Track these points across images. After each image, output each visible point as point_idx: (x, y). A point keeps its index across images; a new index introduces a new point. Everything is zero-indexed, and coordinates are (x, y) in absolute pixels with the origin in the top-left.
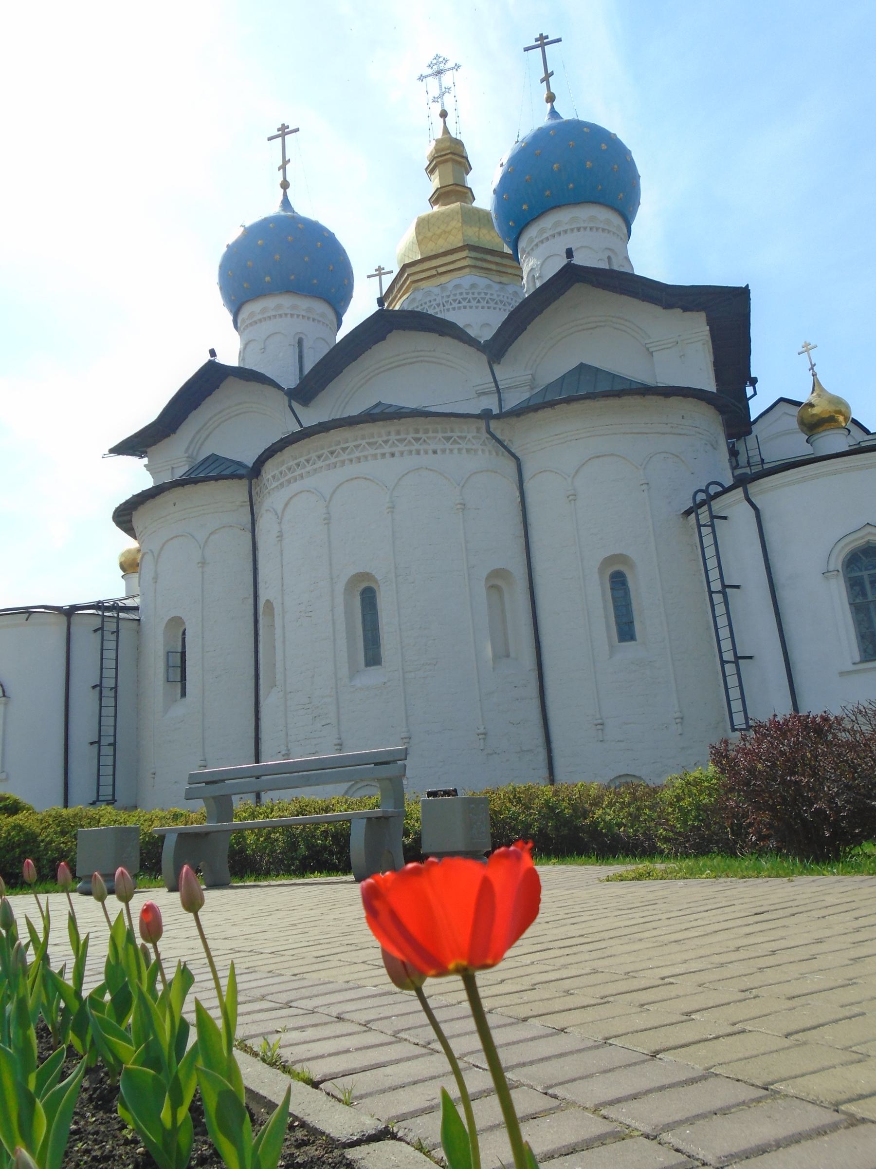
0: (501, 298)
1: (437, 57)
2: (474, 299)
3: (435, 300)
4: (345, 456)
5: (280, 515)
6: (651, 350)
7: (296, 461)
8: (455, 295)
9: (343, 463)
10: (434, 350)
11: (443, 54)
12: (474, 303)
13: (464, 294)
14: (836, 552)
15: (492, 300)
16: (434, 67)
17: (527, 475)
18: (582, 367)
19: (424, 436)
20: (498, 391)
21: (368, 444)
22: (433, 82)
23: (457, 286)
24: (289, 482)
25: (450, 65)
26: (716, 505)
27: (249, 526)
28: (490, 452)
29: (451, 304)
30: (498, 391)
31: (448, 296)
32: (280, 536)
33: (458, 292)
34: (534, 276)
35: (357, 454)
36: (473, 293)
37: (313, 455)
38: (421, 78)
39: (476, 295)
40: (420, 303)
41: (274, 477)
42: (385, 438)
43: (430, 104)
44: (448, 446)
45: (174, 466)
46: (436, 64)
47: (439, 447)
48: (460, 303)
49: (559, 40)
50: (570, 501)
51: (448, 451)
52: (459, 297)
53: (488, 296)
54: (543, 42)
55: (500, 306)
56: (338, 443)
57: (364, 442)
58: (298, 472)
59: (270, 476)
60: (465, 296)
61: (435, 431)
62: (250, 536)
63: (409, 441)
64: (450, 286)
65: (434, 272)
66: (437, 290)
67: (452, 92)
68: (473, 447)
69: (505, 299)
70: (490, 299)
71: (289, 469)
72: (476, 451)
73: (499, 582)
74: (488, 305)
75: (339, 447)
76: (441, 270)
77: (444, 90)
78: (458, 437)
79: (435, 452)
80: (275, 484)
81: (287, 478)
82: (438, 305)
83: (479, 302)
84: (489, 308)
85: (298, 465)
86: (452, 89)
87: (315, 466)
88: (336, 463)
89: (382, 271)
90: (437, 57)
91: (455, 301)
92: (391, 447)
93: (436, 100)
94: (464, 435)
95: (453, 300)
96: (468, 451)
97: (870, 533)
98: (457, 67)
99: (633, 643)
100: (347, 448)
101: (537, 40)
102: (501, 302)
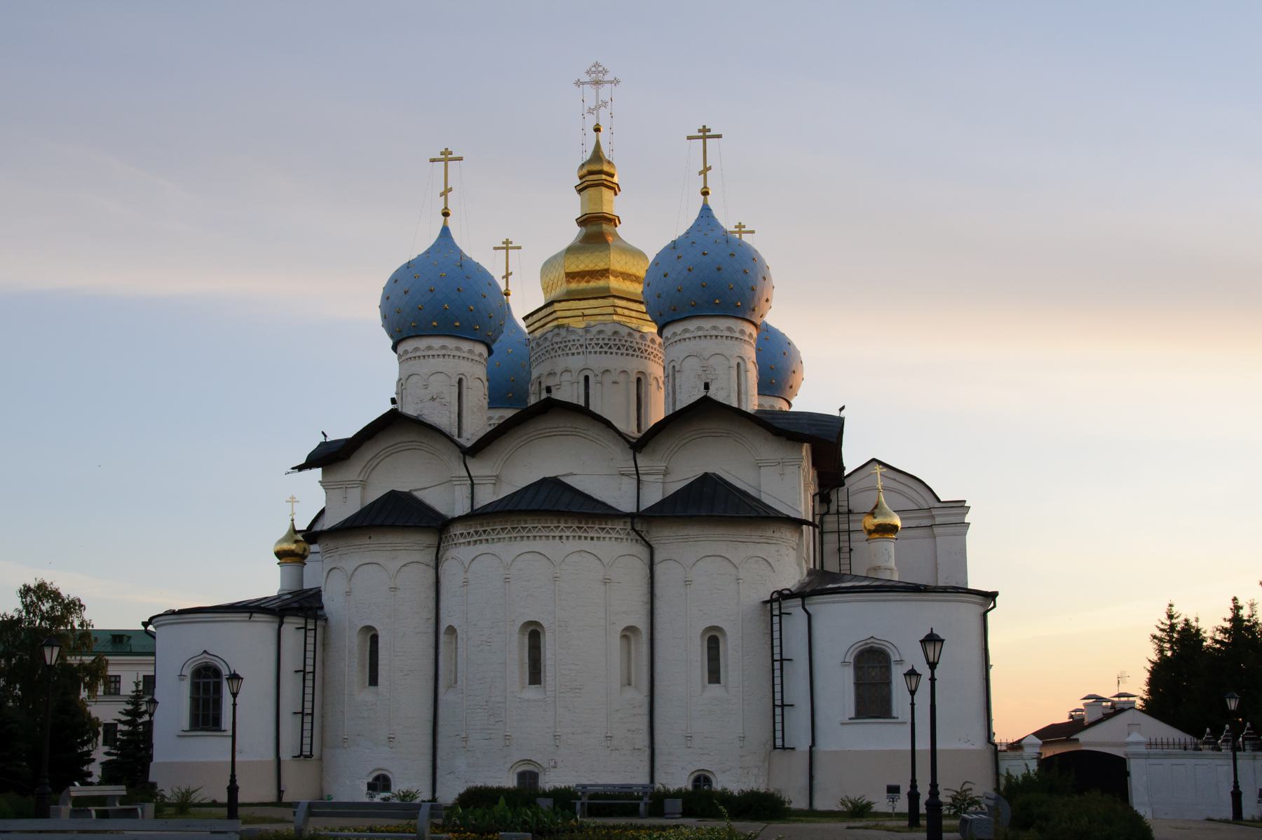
0: (640, 346)
1: (597, 65)
2: (615, 345)
3: (579, 340)
4: (524, 534)
5: (467, 567)
6: (760, 465)
7: (483, 529)
8: (598, 339)
9: (522, 537)
10: (588, 430)
11: (605, 64)
12: (614, 350)
13: (606, 339)
14: (851, 651)
15: (632, 347)
16: (593, 75)
17: (657, 558)
18: (706, 476)
19: (585, 527)
20: (638, 474)
21: (543, 527)
22: (589, 90)
23: (600, 332)
24: (475, 542)
25: (608, 77)
26: (785, 604)
27: (433, 563)
28: (632, 540)
29: (593, 347)
30: (638, 474)
31: (591, 339)
32: (466, 583)
33: (601, 336)
34: (674, 367)
35: (535, 534)
36: (615, 340)
37: (499, 527)
38: (579, 83)
39: (617, 342)
40: (565, 339)
41: (462, 534)
42: (556, 525)
43: (585, 114)
44: (602, 535)
45: (347, 486)
46: (594, 72)
47: (596, 535)
48: (601, 347)
49: (719, 136)
50: (686, 585)
51: (602, 539)
52: (601, 342)
53: (628, 344)
54: (705, 134)
55: (638, 353)
56: (519, 522)
57: (540, 526)
58: (484, 537)
59: (458, 533)
60: (606, 341)
61: (593, 523)
62: (432, 572)
63: (574, 529)
64: (594, 331)
65: (579, 313)
66: (581, 332)
67: (609, 107)
68: (620, 537)
69: (643, 347)
70: (630, 346)
71: (476, 532)
72: (621, 539)
73: (628, 633)
74: (628, 352)
75: (519, 526)
76: (587, 312)
77: (600, 103)
78: (610, 528)
79: (592, 538)
80: (462, 540)
81: (474, 539)
82: (581, 346)
83: (619, 348)
84: (627, 355)
85: (485, 531)
86: (609, 104)
87: (499, 536)
88: (516, 538)
89: (510, 245)
90: (597, 65)
91: (597, 344)
92: (560, 532)
93: (591, 111)
94: (614, 527)
95: (596, 344)
96: (616, 539)
97: (872, 643)
98: (616, 82)
99: (717, 685)
100: (527, 527)
101: (700, 131)
102: (639, 349)
